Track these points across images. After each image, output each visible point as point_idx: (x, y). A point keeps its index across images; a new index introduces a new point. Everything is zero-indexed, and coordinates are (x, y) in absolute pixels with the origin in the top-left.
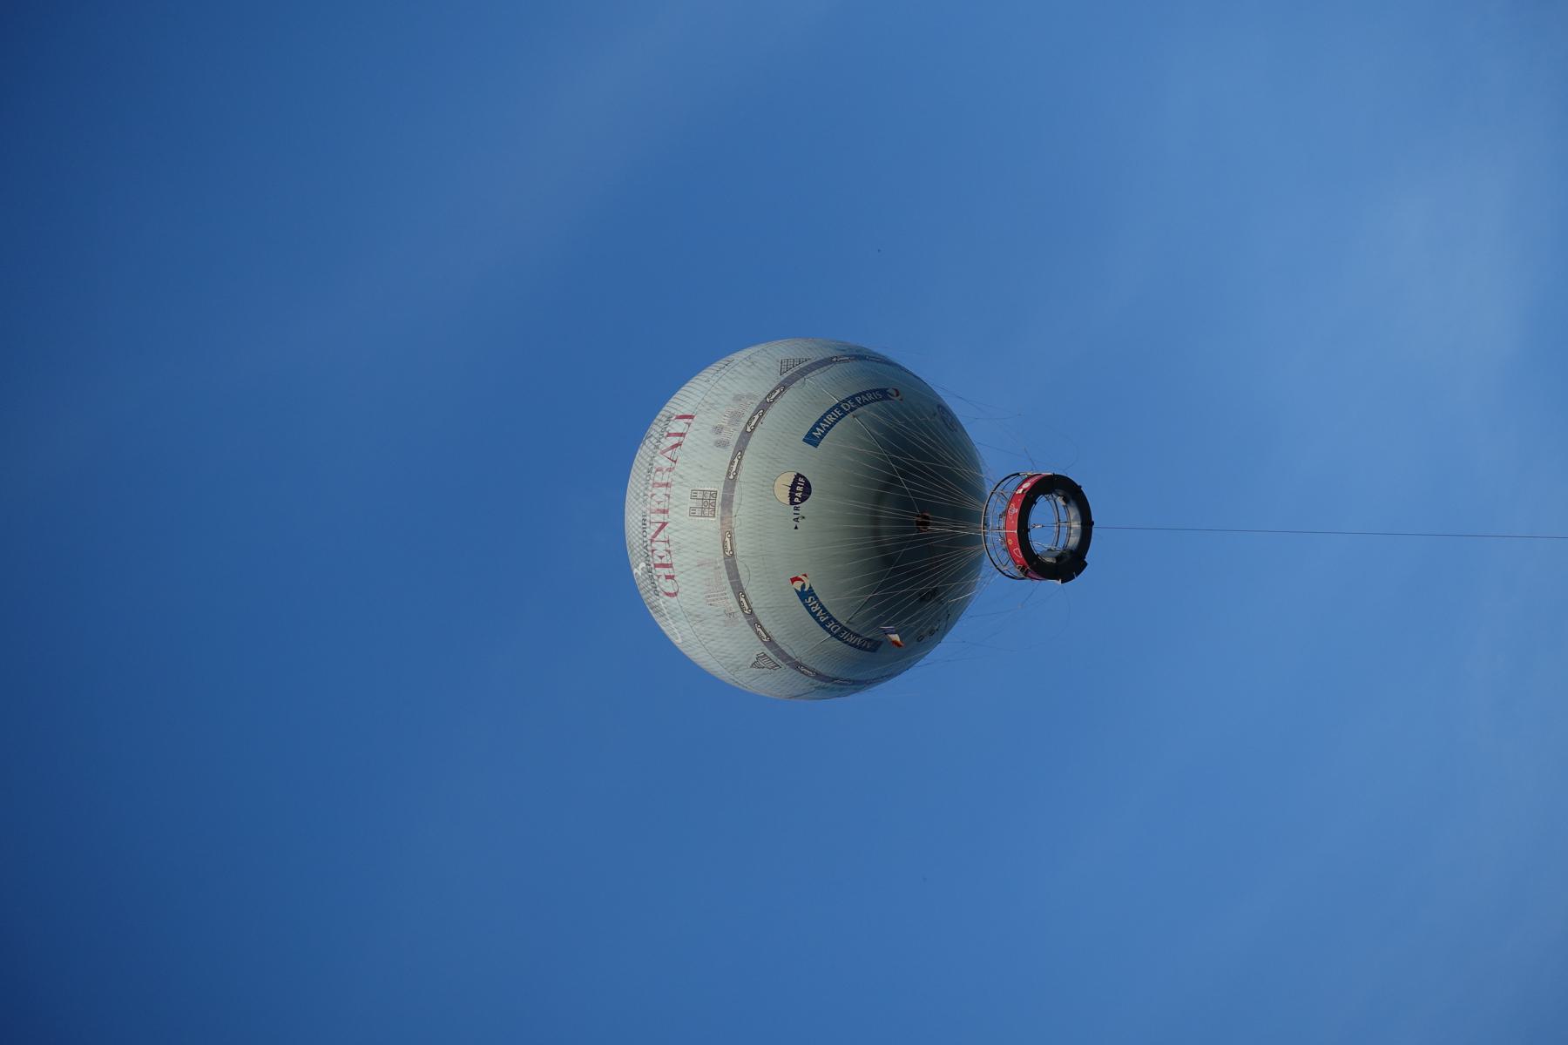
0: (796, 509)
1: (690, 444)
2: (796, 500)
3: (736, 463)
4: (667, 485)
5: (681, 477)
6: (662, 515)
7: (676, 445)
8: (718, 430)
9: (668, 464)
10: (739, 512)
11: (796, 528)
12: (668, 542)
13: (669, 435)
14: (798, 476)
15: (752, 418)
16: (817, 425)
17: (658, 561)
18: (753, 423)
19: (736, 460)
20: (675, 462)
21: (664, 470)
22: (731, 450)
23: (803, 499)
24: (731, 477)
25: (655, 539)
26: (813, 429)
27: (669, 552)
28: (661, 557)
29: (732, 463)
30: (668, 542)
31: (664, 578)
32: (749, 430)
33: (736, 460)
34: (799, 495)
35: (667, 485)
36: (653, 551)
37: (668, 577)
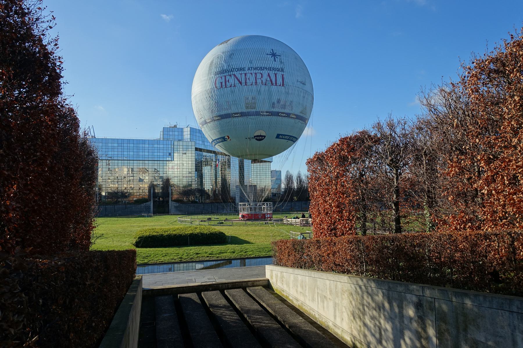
0: (253, 138)
1: (272, 90)
2: (256, 138)
3: (267, 114)
4: (256, 83)
5: (260, 90)
6: (244, 82)
7: (272, 83)
8: (279, 101)
9: (264, 81)
10: (249, 119)
11: (246, 138)
12: (235, 86)
13: (276, 75)
14: (265, 137)
15: (283, 113)
16: (283, 135)
17: (227, 80)
18: (282, 115)
19: (268, 114)
20: (265, 85)
21: (262, 79)
22: (272, 110)
23: (256, 139)
24: (261, 114)
26: (282, 135)
27: (231, 86)
28: (228, 81)
29: (267, 112)
30: (235, 86)
32: (280, 114)
33: (268, 114)
34: (258, 138)
35: (256, 83)
36: (230, 75)
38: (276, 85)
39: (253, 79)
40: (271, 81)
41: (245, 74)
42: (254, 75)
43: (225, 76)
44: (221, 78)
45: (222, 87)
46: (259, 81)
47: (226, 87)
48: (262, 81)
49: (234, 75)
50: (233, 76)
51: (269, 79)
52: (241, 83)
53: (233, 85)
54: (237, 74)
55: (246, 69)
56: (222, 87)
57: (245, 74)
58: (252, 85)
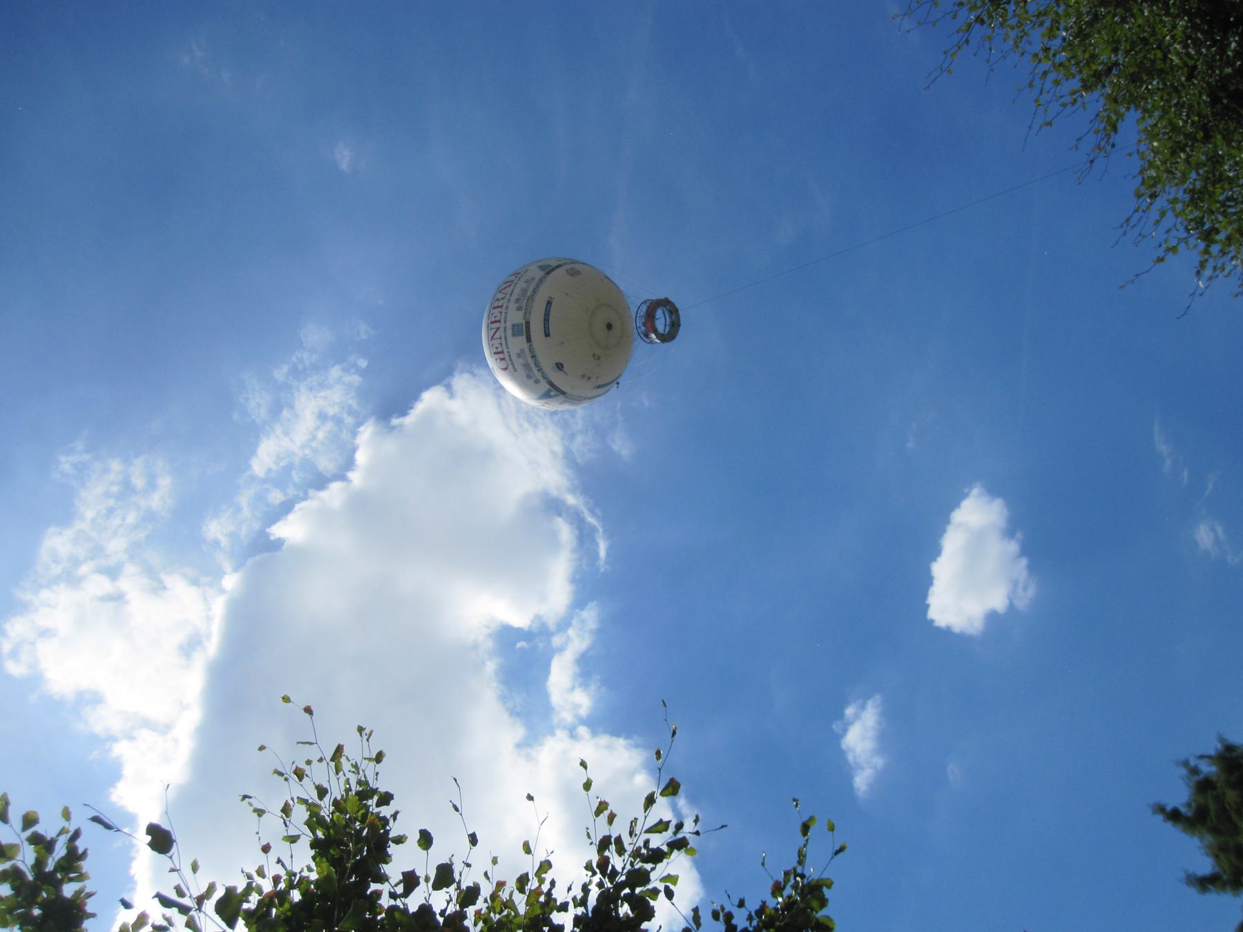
12: (500, 338)
27: (501, 344)
38: (512, 281)
39: (496, 312)
40: (505, 288)
42: (494, 311)
46: (501, 303)
48: (501, 299)
52: (498, 329)
53: (499, 341)
56: (503, 359)
58: (501, 312)
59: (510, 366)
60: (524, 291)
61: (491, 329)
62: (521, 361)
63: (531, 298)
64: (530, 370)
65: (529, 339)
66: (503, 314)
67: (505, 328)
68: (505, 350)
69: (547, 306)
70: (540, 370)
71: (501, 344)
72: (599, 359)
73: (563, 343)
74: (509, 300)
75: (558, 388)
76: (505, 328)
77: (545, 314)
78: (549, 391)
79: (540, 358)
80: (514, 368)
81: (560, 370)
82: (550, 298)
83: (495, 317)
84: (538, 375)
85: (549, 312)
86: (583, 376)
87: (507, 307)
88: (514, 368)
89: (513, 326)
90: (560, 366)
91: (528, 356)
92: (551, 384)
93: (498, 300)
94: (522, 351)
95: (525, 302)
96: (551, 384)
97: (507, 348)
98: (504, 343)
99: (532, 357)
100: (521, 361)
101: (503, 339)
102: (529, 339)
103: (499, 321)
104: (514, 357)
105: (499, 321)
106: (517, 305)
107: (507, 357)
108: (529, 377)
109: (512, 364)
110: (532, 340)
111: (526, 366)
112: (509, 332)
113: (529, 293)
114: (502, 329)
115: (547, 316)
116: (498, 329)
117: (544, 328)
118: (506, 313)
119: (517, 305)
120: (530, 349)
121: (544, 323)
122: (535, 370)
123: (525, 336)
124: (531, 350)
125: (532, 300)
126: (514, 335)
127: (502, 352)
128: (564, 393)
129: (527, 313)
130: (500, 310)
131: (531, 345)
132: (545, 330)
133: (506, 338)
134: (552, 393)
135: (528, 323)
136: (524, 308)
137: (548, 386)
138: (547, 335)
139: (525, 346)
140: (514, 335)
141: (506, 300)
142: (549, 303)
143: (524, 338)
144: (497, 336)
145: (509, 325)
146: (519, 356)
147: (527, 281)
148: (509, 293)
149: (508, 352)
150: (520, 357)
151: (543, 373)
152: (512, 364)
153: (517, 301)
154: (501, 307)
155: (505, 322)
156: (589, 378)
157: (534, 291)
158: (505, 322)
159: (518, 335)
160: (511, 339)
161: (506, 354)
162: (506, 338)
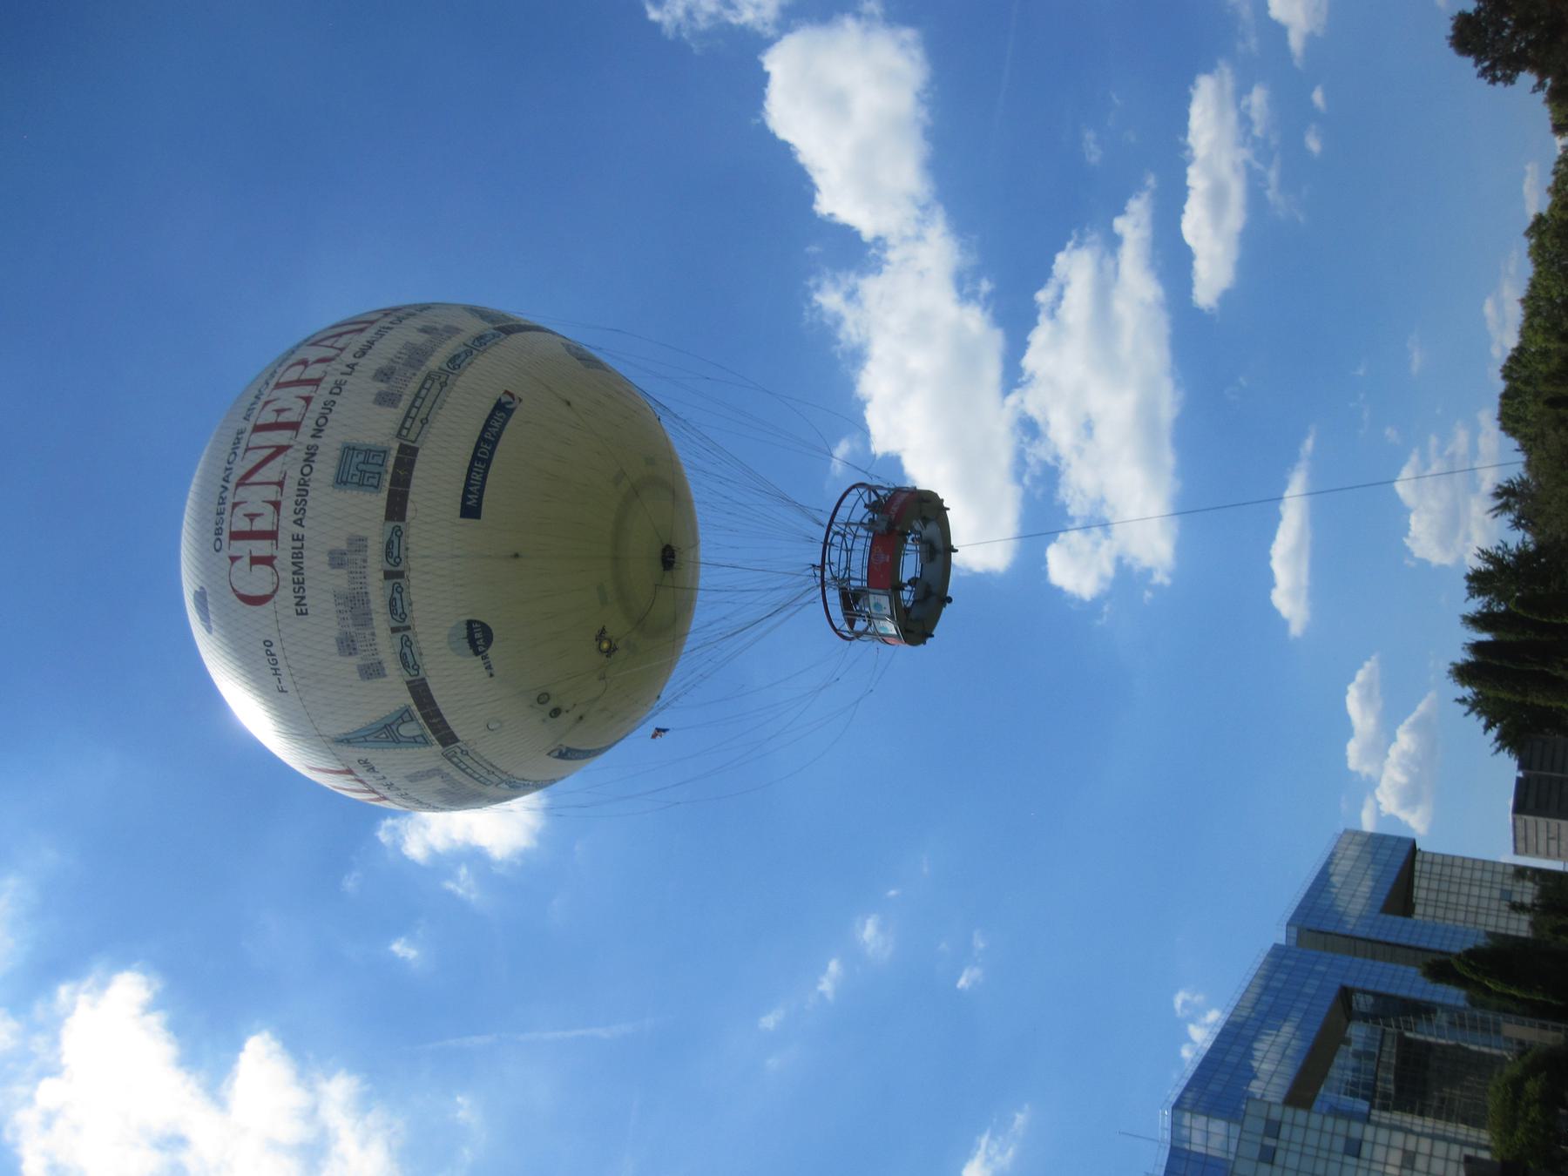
12: (280, 484)
17: (243, 525)
21: (310, 362)
25: (247, 482)
27: (276, 505)
28: (252, 517)
31: (247, 560)
37: (255, 561)
39: (289, 399)
41: (258, 428)
42: (277, 393)
43: (236, 536)
44: (233, 559)
45: (268, 561)
46: (314, 372)
47: (272, 535)
49: (242, 482)
50: (243, 493)
51: (328, 343)
52: (280, 450)
53: (271, 493)
54: (239, 470)
55: (242, 425)
56: (268, 561)
57: (258, 428)
58: (308, 400)
59: (286, 595)
60: (416, 356)
61: (248, 449)
62: (340, 580)
63: (441, 381)
64: (364, 619)
65: (396, 508)
66: (316, 407)
67: (311, 454)
68: (287, 528)
69: (491, 416)
70: (401, 627)
71: (276, 505)
72: (610, 652)
73: (517, 556)
74: (352, 366)
75: (438, 714)
76: (311, 454)
77: (481, 439)
78: (404, 716)
79: (418, 590)
80: (300, 601)
81: (477, 653)
82: (507, 392)
83: (279, 411)
84: (386, 647)
85: (498, 436)
86: (543, 698)
87: (339, 386)
88: (300, 601)
89: (349, 450)
90: (478, 637)
91: (375, 564)
92: (420, 692)
93: (305, 363)
94: (358, 543)
95: (413, 386)
96: (420, 692)
97: (299, 522)
98: (288, 506)
99: (388, 575)
100: (340, 580)
101: (291, 487)
102: (396, 508)
103: (294, 426)
104: (315, 562)
105: (294, 426)
106: (383, 386)
107: (284, 556)
108: (347, 645)
109: (299, 585)
110: (409, 514)
111: (355, 605)
112: (325, 468)
113: (435, 362)
114: (297, 455)
115: (486, 447)
116: (280, 450)
117: (468, 477)
118: (329, 406)
119: (383, 386)
120: (389, 546)
121: (470, 470)
122: (381, 622)
123: (384, 494)
124: (391, 550)
125: (443, 385)
126: (341, 481)
127: (272, 535)
128: (447, 737)
129: (416, 418)
130: (305, 391)
131: (398, 532)
132: (466, 491)
133: (303, 486)
134: (407, 730)
135: (407, 457)
136: (404, 405)
137: (407, 699)
138: (470, 509)
139: (375, 530)
140: (341, 481)
141: (338, 366)
142: (503, 409)
143: (378, 501)
144: (271, 472)
145: (330, 448)
146: (336, 560)
147: (424, 330)
148: (355, 347)
149: (296, 538)
150: (341, 565)
151: (407, 643)
152: (299, 585)
153: (384, 375)
154: (315, 382)
155: (318, 432)
156: (556, 712)
157: (455, 362)
158: (318, 432)
159: (360, 485)
160: (323, 495)
161: (284, 538)
162: (303, 486)
